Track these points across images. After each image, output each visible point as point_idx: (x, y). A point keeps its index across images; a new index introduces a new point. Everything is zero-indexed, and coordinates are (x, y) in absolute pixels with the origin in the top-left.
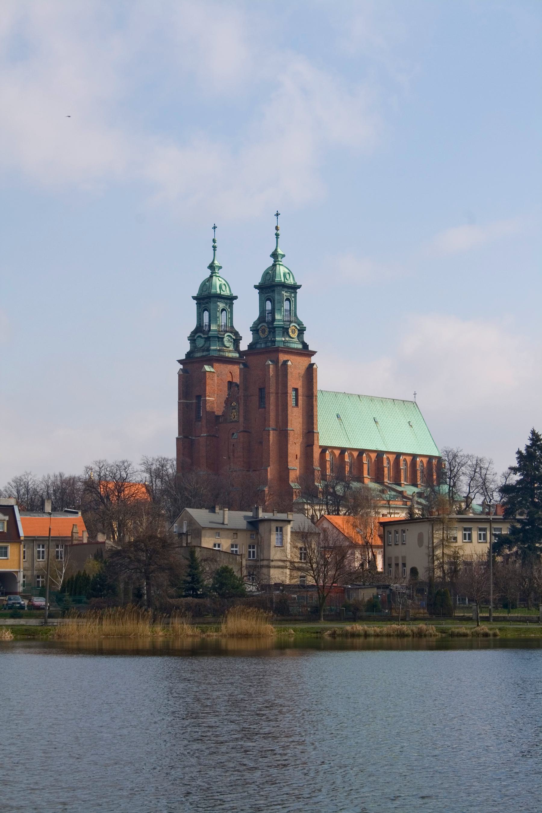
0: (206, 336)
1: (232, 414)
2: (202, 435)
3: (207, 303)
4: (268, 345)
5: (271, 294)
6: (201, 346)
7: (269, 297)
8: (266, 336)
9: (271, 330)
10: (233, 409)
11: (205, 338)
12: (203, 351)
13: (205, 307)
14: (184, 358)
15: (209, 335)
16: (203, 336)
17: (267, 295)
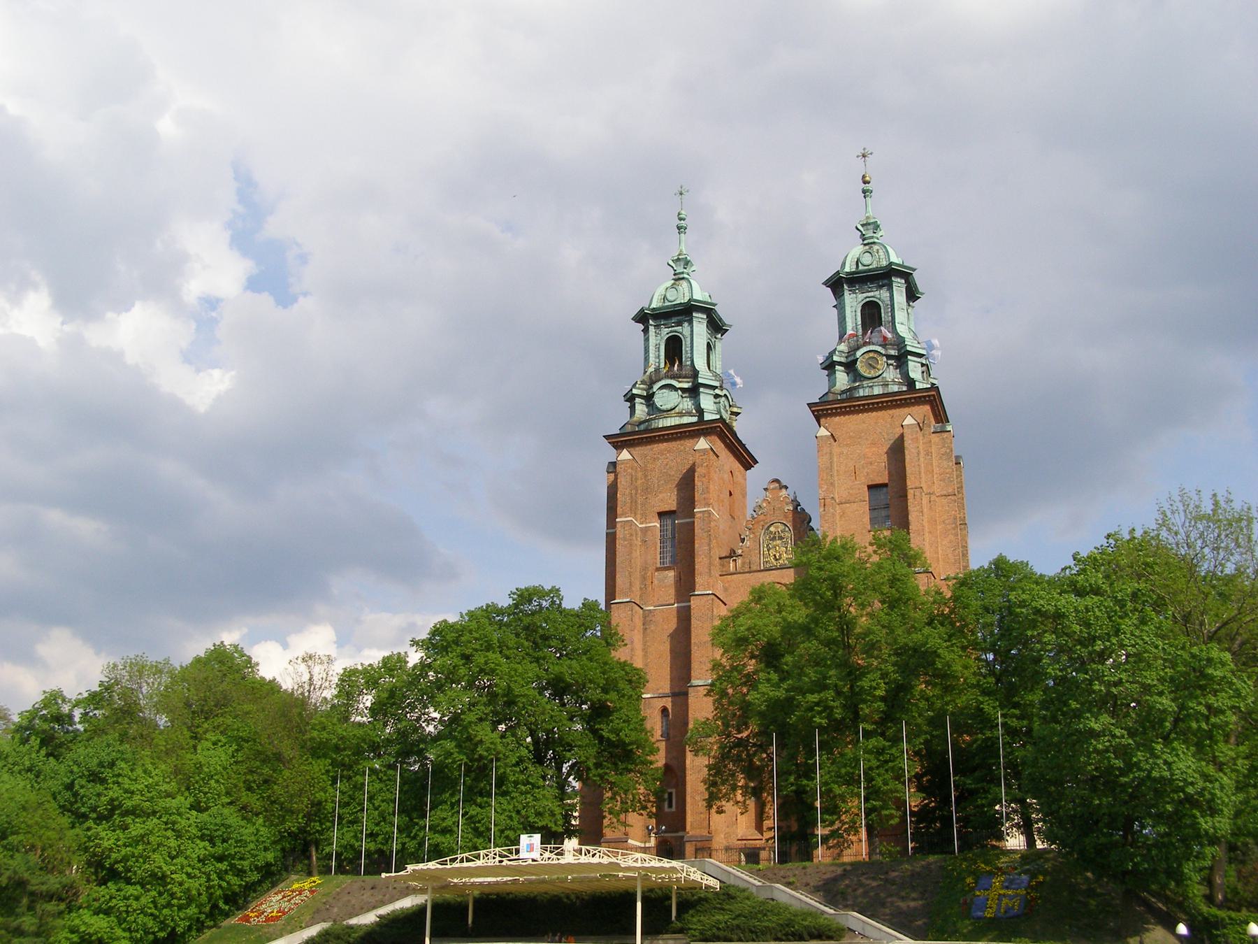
0: (686, 386)
1: (772, 552)
2: (696, 593)
3: (679, 324)
4: (890, 391)
5: (877, 293)
6: (669, 406)
7: (871, 299)
8: (880, 372)
9: (890, 362)
10: (774, 539)
11: (680, 388)
12: (681, 414)
13: (671, 332)
14: (618, 432)
15: (700, 381)
16: (678, 385)
17: (865, 295)
